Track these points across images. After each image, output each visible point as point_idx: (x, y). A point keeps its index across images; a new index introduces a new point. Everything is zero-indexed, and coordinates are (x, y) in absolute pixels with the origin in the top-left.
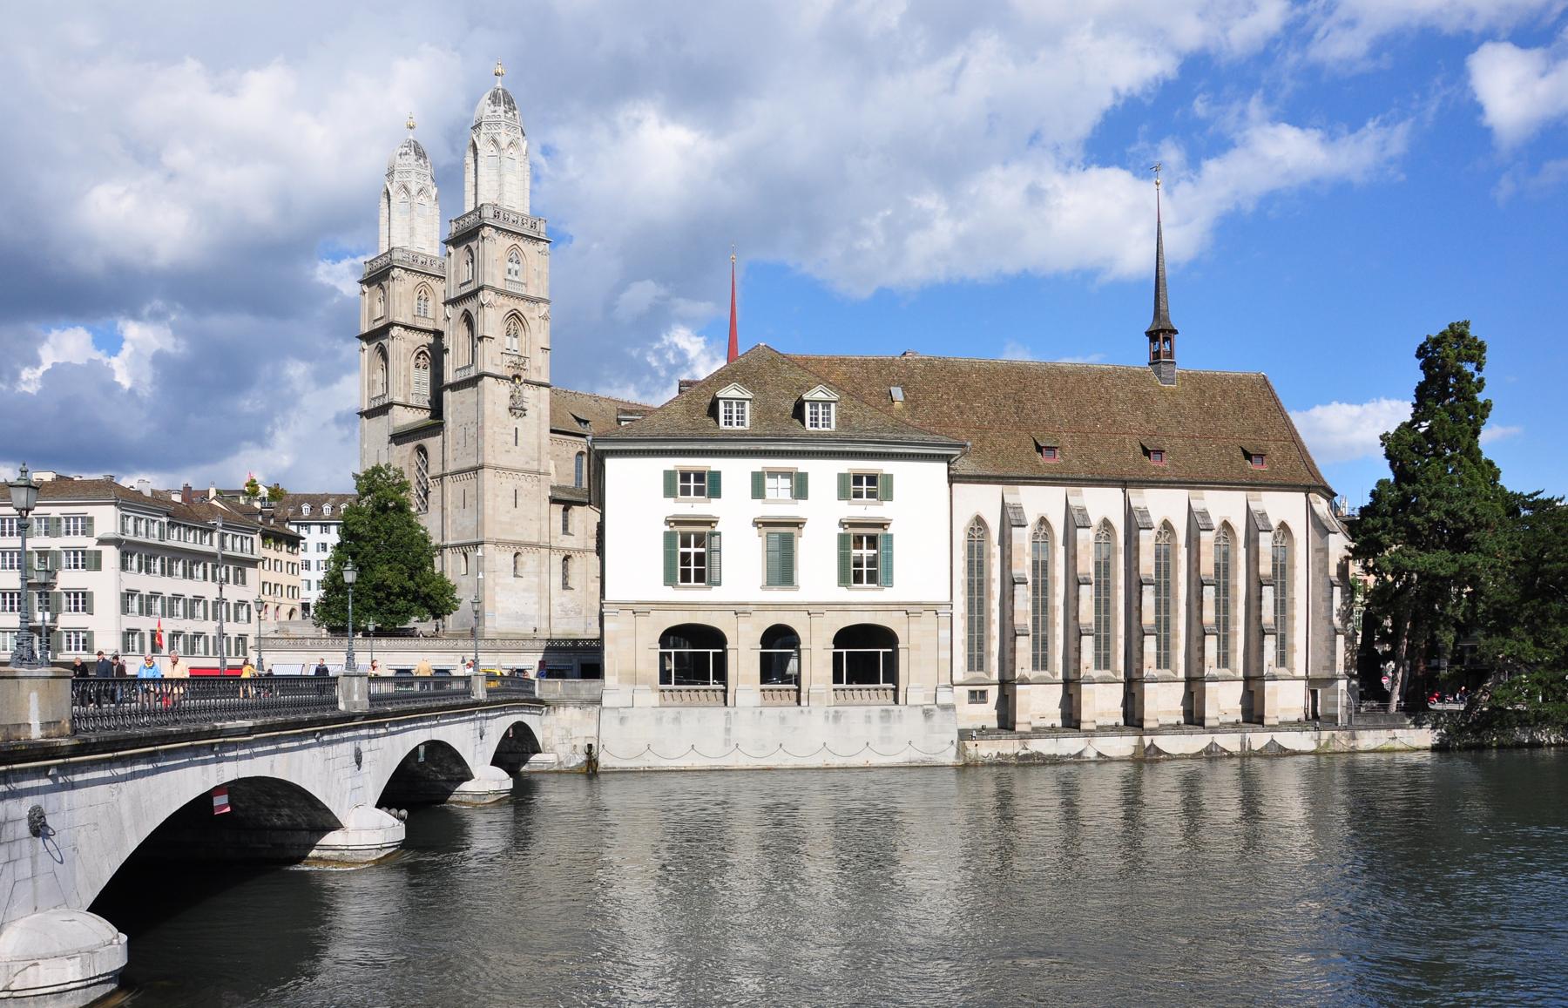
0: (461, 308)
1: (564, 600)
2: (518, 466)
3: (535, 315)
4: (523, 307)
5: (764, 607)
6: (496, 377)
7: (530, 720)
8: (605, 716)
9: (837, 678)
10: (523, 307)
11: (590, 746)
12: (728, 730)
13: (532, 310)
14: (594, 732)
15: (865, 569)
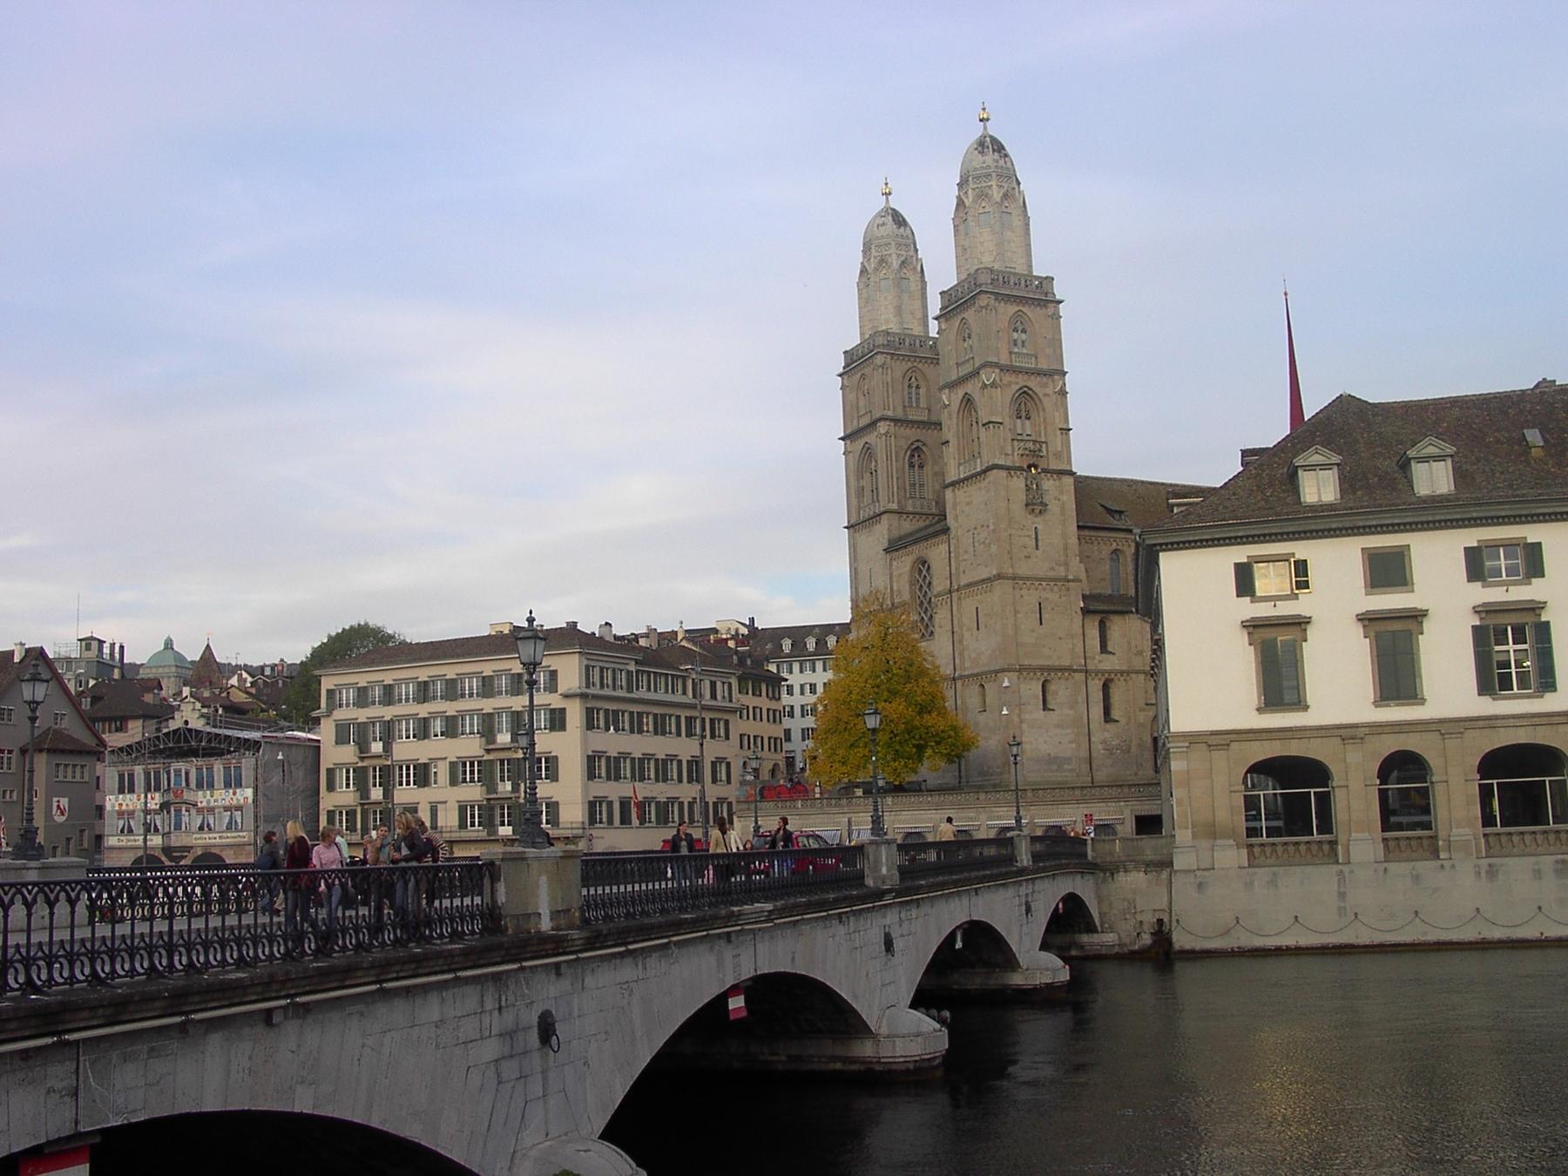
0: (960, 393)
1: (1107, 735)
2: (1041, 574)
3: (1049, 390)
4: (1033, 383)
5: (1378, 729)
6: (1008, 468)
7: (1083, 887)
8: (1178, 881)
9: (1488, 820)
10: (1033, 383)
11: (1160, 921)
12: (1342, 895)
13: (1045, 385)
14: (1164, 904)
15: (1513, 670)
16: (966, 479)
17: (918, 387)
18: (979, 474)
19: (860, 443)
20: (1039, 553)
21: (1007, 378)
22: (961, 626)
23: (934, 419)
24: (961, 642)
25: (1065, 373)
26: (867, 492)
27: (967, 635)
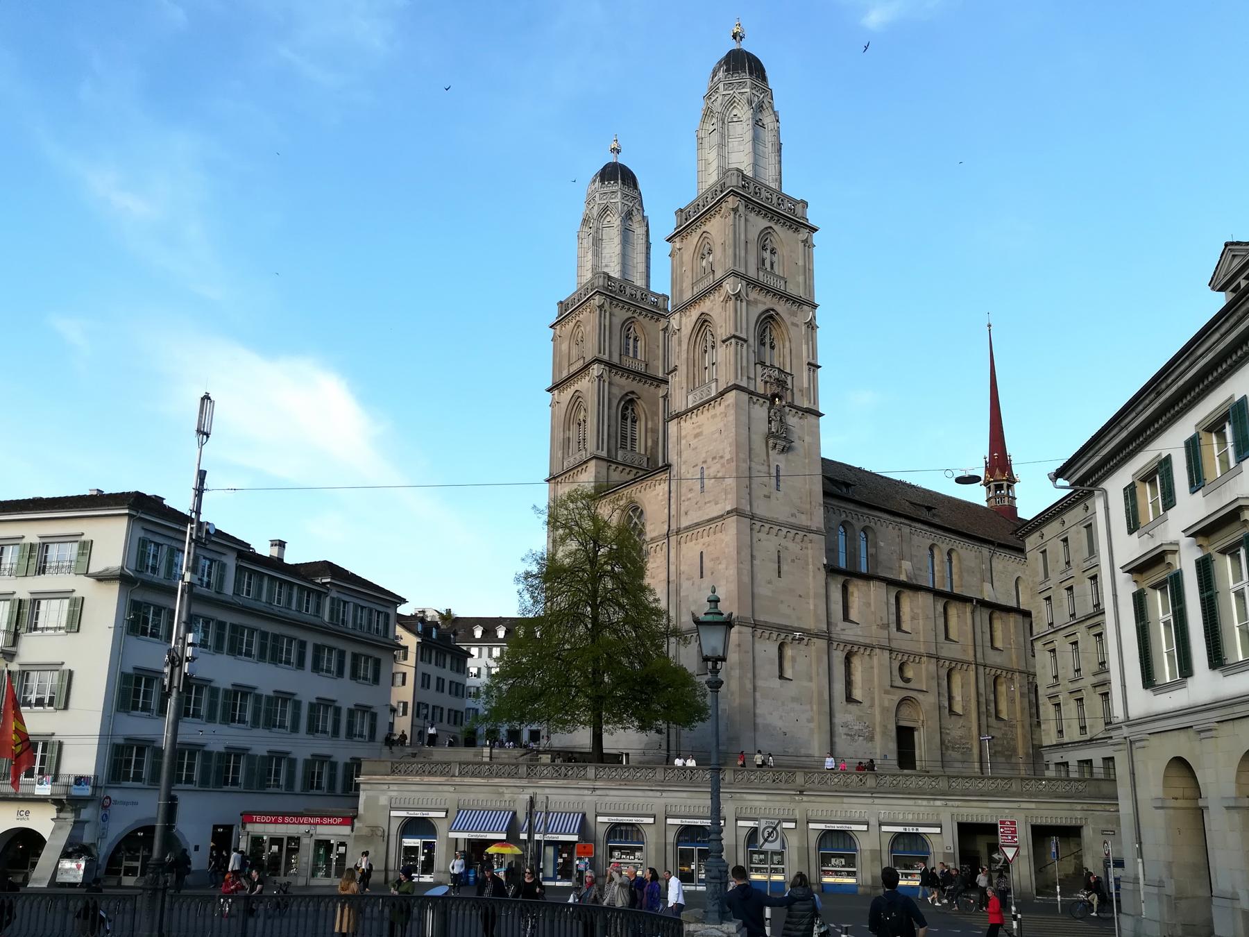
0: (694, 314)
2: (782, 518)
6: (751, 393)
13: (794, 314)
16: (697, 407)
17: (636, 340)
18: (714, 399)
19: (567, 394)
20: (780, 494)
21: (754, 295)
22: (679, 574)
23: (650, 372)
24: (678, 592)
25: (815, 306)
26: (573, 445)
27: (685, 585)
